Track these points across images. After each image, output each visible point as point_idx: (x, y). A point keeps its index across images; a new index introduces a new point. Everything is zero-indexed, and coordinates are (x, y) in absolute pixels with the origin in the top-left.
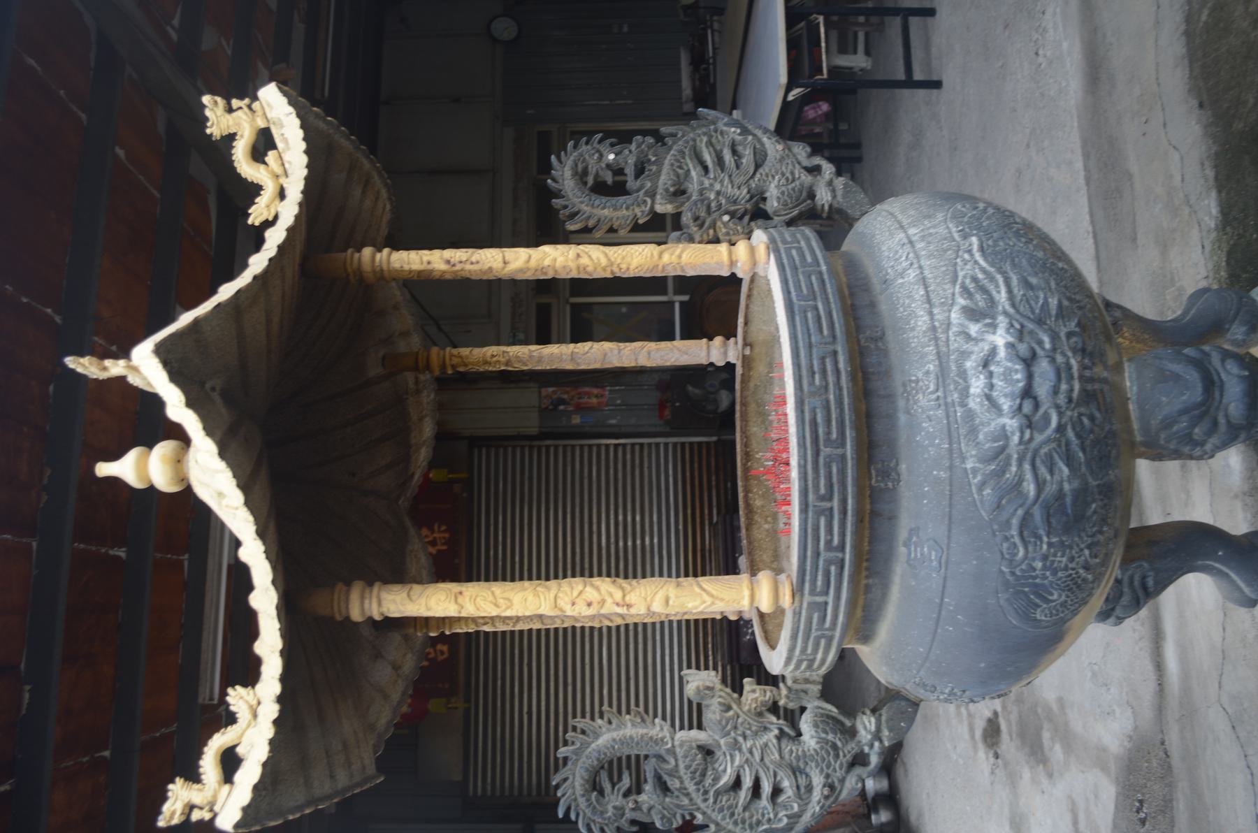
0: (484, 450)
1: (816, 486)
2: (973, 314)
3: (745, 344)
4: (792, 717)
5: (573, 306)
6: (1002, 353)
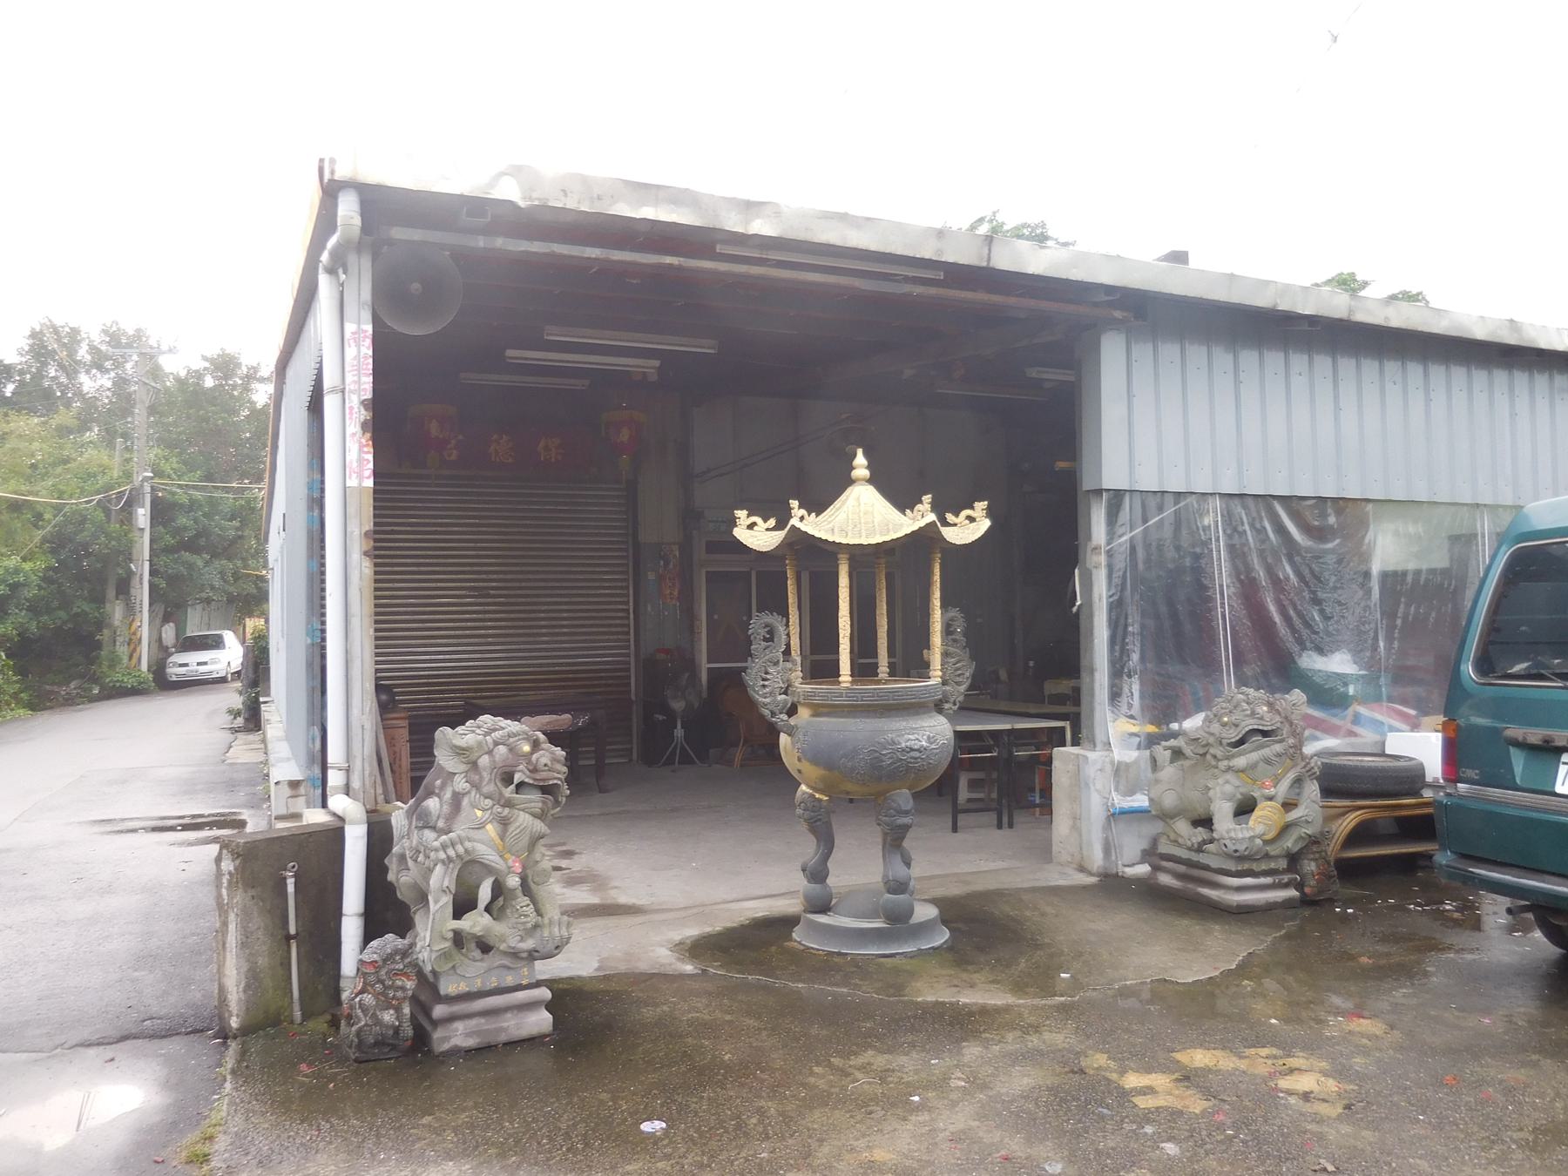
4: (785, 693)
5: (749, 573)
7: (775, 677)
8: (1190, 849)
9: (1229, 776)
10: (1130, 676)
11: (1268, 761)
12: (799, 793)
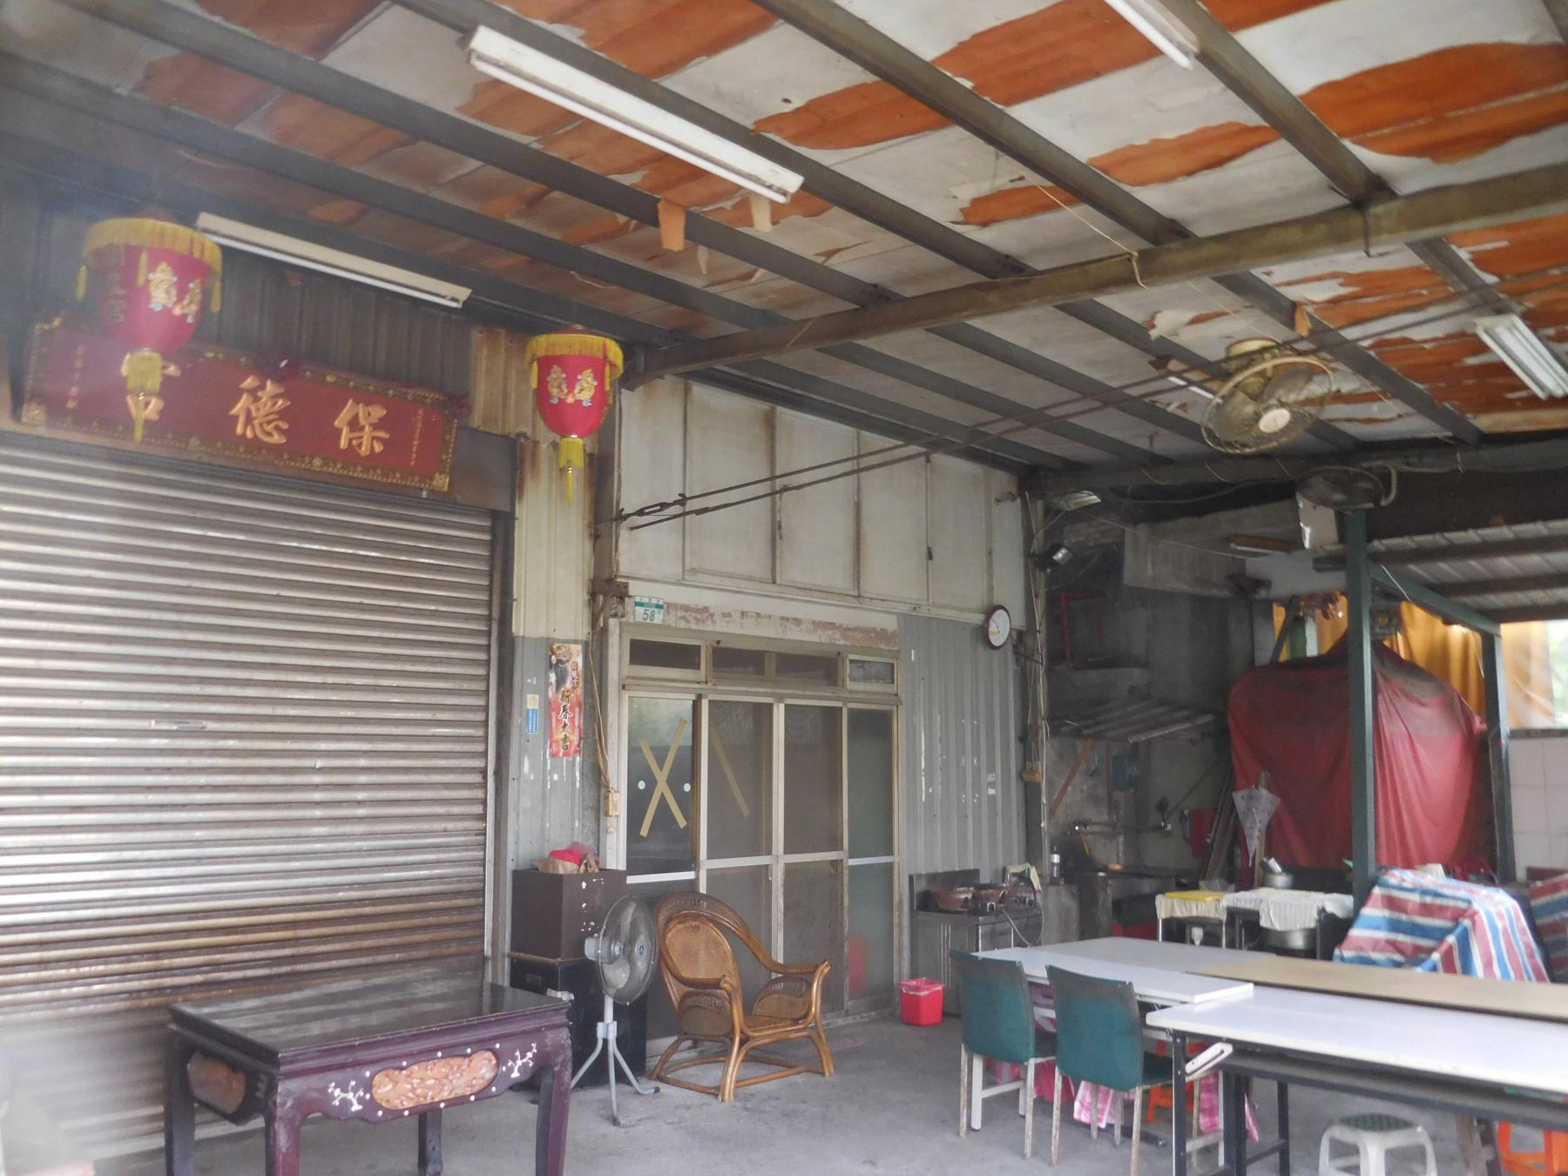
0: (487, 537)
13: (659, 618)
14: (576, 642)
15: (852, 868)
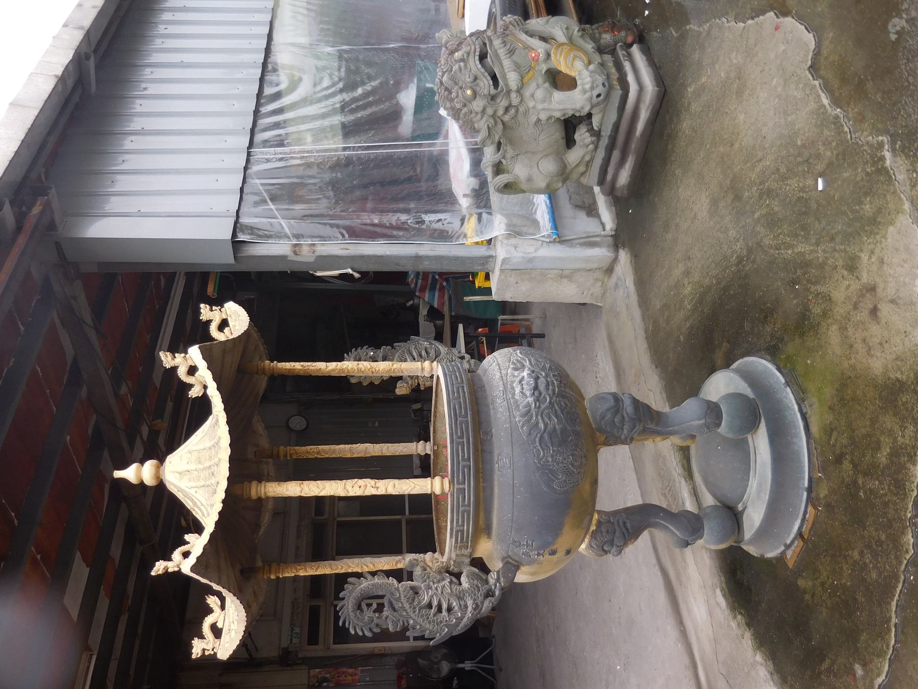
1: (457, 432)
2: (516, 369)
3: (434, 444)
4: (458, 576)
6: (526, 377)
7: (430, 594)
8: (596, 148)
9: (527, 93)
10: (423, 222)
11: (511, 52)
12: (584, 553)
13: (297, 630)
14: (309, 673)
15: (410, 514)
